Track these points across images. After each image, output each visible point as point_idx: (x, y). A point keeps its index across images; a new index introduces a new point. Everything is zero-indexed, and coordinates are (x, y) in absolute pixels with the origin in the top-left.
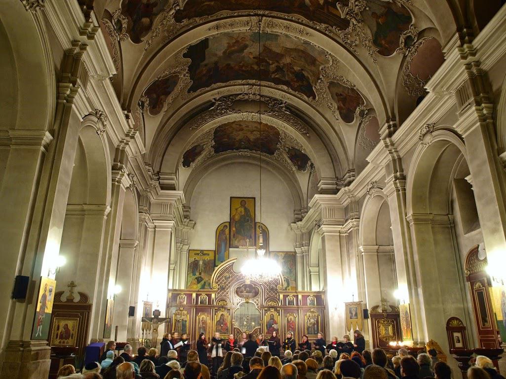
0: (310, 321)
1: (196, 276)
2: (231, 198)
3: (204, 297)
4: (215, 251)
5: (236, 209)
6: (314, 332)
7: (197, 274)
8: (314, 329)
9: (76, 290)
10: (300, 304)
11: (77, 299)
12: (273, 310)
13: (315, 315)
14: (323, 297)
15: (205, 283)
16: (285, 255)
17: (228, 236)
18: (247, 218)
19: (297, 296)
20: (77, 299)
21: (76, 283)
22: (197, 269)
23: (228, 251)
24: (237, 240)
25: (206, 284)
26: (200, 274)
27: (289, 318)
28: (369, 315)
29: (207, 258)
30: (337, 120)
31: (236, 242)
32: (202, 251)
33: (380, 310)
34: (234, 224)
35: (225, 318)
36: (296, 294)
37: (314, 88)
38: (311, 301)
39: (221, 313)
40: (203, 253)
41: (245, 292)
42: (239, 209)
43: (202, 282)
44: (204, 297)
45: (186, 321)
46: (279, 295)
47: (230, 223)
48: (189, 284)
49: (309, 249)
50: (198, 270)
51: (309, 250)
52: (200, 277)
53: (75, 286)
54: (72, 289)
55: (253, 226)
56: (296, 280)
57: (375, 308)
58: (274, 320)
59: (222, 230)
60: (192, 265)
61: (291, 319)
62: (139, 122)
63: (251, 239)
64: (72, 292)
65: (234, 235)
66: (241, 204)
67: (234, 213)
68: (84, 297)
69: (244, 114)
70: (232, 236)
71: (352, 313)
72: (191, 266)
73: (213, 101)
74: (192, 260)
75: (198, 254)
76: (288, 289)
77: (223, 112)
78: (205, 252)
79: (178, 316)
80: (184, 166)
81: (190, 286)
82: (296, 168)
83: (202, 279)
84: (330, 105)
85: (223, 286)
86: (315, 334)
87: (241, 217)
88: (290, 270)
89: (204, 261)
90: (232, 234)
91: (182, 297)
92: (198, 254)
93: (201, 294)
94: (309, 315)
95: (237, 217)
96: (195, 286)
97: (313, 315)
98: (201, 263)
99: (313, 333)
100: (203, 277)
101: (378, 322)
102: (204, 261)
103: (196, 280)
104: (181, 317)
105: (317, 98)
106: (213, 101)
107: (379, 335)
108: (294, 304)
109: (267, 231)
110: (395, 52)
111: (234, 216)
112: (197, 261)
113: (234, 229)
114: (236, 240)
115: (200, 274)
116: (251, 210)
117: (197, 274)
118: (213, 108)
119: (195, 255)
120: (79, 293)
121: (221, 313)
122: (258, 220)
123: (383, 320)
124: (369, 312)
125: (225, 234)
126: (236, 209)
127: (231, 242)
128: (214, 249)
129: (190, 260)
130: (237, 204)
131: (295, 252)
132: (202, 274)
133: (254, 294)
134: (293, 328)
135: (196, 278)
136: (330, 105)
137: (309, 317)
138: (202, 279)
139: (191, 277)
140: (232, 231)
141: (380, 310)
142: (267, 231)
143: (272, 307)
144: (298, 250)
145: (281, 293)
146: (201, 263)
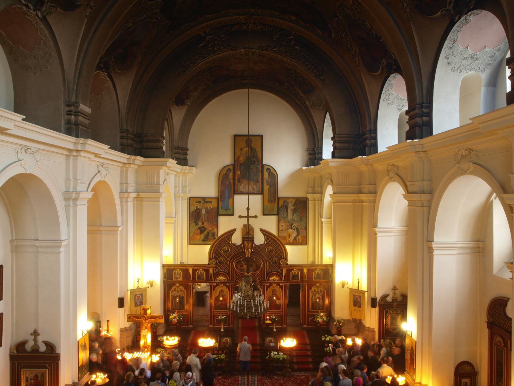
0: (315, 296)
1: (199, 226)
2: (235, 136)
3: (201, 272)
4: (218, 198)
5: (241, 150)
7: (200, 224)
9: (40, 339)
10: (305, 278)
11: (43, 348)
13: (321, 290)
14: (330, 271)
15: (208, 233)
16: (296, 201)
17: (232, 181)
18: (253, 159)
20: (43, 348)
21: (39, 332)
22: (199, 219)
23: (232, 199)
24: (243, 185)
25: (210, 234)
26: (203, 223)
28: (378, 304)
29: (209, 206)
30: (358, 66)
31: (241, 187)
32: (204, 199)
33: (389, 299)
34: (239, 167)
35: (224, 293)
37: (329, 25)
38: (317, 275)
39: (220, 288)
40: (204, 200)
42: (245, 149)
43: (206, 232)
44: (201, 272)
45: (183, 297)
46: (282, 270)
47: (234, 165)
48: (192, 234)
49: (322, 196)
50: (201, 219)
51: (321, 198)
52: (203, 227)
53: (39, 335)
54: (35, 338)
55: (260, 169)
56: (306, 229)
57: (385, 297)
59: (226, 174)
60: (194, 214)
62: (106, 83)
63: (258, 184)
64: (35, 340)
65: (239, 178)
66: (246, 143)
67: (238, 152)
68: (51, 347)
69: (242, 50)
70: (237, 182)
72: (192, 215)
73: (203, 34)
74: (194, 208)
75: (200, 202)
76: (297, 238)
77: (216, 49)
78: (207, 200)
79: (174, 292)
80: (178, 106)
81: (192, 236)
82: (309, 102)
83: (205, 229)
84: (349, 47)
85: (221, 260)
87: (248, 158)
88: (301, 218)
89: (206, 209)
90: (237, 178)
91: (178, 272)
92: (200, 202)
93: (198, 269)
94: (315, 290)
95: (242, 159)
96: (198, 237)
97: (319, 290)
98: (203, 211)
100: (206, 227)
101: (387, 312)
102: (206, 209)
103: (199, 230)
104: (178, 293)
105: (334, 35)
106: (203, 34)
107: (386, 326)
108: (298, 279)
109: (276, 175)
110: (440, 13)
111: (239, 157)
112: (198, 209)
113: (239, 173)
114: (241, 185)
115: (203, 223)
116: (258, 150)
117: (200, 224)
118: (203, 44)
119: (196, 202)
120: (44, 342)
121: (220, 288)
122: (267, 160)
123: (392, 309)
124: (378, 300)
125: (229, 179)
126: (241, 150)
127: (236, 188)
128: (217, 196)
129: (191, 209)
130: (242, 144)
131: (307, 199)
132: (205, 224)
133: (255, 268)
135: (199, 228)
136: (349, 47)
137: (315, 291)
138: (205, 229)
139: (193, 227)
140: (236, 175)
141: (389, 299)
142: (276, 175)
144: (310, 196)
145: (285, 267)
146: (203, 211)
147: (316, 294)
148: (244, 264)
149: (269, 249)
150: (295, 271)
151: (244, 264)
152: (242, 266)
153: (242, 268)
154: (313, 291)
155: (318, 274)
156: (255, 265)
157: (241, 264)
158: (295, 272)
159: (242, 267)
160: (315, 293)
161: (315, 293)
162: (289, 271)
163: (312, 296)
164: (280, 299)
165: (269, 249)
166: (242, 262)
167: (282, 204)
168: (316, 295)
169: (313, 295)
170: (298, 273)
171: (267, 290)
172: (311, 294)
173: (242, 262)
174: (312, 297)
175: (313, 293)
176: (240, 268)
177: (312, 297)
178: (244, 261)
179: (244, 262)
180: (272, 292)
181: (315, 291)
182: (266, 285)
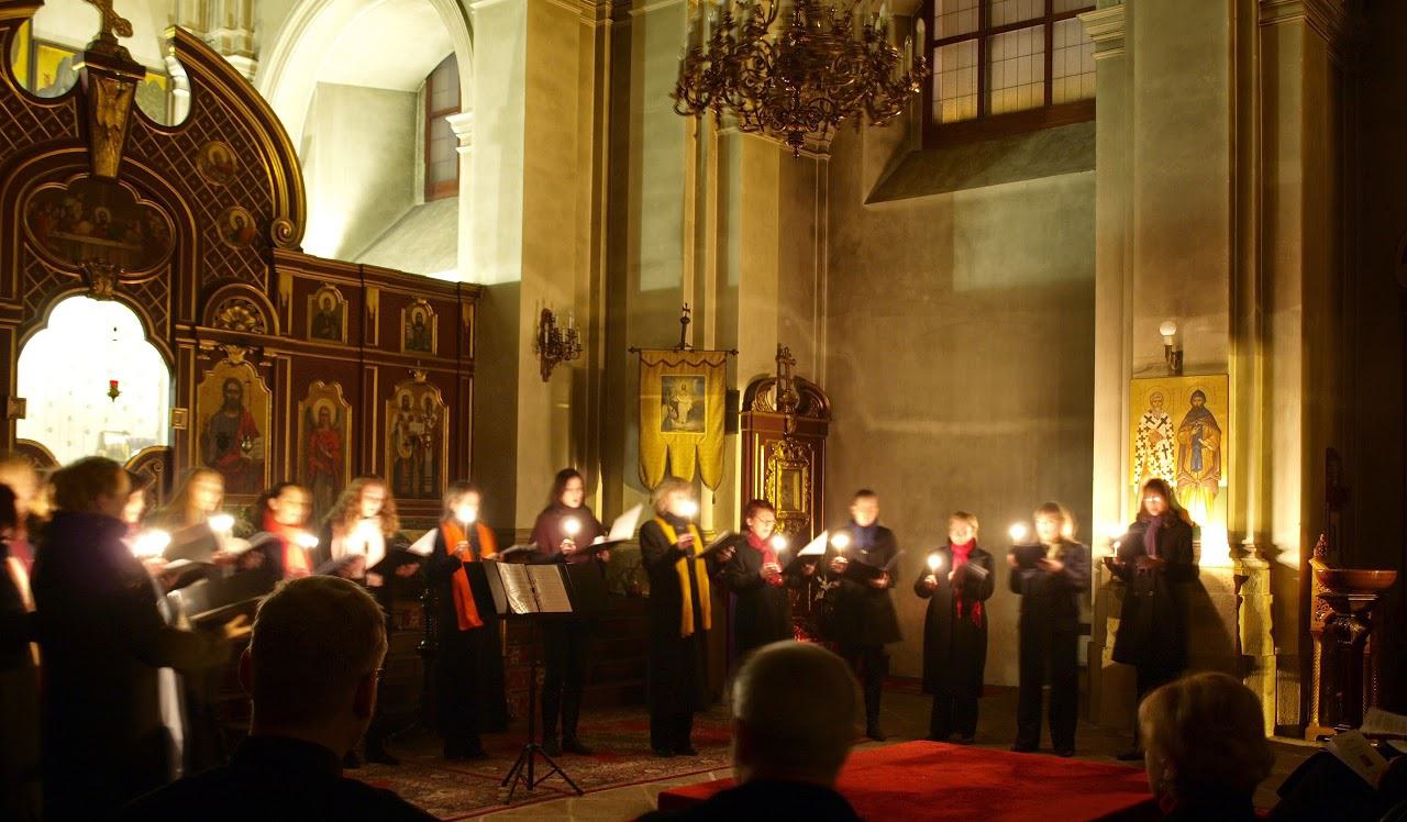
0: (406, 428)
6: (421, 488)
8: (422, 471)
12: (237, 355)
19: (362, 292)
27: (316, 408)
36: (356, 283)
38: (414, 328)
41: (86, 226)
58: (242, 409)
61: (324, 412)
71: (675, 406)
86: (424, 496)
94: (405, 399)
99: (416, 486)
108: (339, 338)
134: (330, 461)
143: (241, 342)
147: (411, 419)
148: (78, 216)
149: (212, 159)
150: (331, 298)
151: (78, 216)
152: (66, 225)
153: (69, 236)
154: (401, 405)
155: (419, 324)
156: (138, 230)
157: (63, 213)
158: (327, 301)
159: (71, 231)
160: (406, 415)
161: (406, 415)
162: (303, 288)
163: (393, 430)
164: (258, 435)
165: (212, 159)
166: (69, 202)
167: (52, 82)
168: (411, 424)
169: (397, 425)
170: (339, 306)
171: (199, 379)
172: (391, 417)
173: (69, 202)
174: (397, 432)
175: (401, 418)
176: (57, 234)
177: (397, 432)
178: (80, 196)
179: (79, 204)
180: (221, 391)
181: (406, 408)
182: (199, 352)
